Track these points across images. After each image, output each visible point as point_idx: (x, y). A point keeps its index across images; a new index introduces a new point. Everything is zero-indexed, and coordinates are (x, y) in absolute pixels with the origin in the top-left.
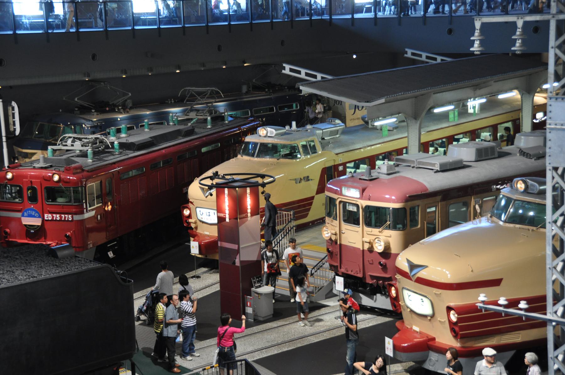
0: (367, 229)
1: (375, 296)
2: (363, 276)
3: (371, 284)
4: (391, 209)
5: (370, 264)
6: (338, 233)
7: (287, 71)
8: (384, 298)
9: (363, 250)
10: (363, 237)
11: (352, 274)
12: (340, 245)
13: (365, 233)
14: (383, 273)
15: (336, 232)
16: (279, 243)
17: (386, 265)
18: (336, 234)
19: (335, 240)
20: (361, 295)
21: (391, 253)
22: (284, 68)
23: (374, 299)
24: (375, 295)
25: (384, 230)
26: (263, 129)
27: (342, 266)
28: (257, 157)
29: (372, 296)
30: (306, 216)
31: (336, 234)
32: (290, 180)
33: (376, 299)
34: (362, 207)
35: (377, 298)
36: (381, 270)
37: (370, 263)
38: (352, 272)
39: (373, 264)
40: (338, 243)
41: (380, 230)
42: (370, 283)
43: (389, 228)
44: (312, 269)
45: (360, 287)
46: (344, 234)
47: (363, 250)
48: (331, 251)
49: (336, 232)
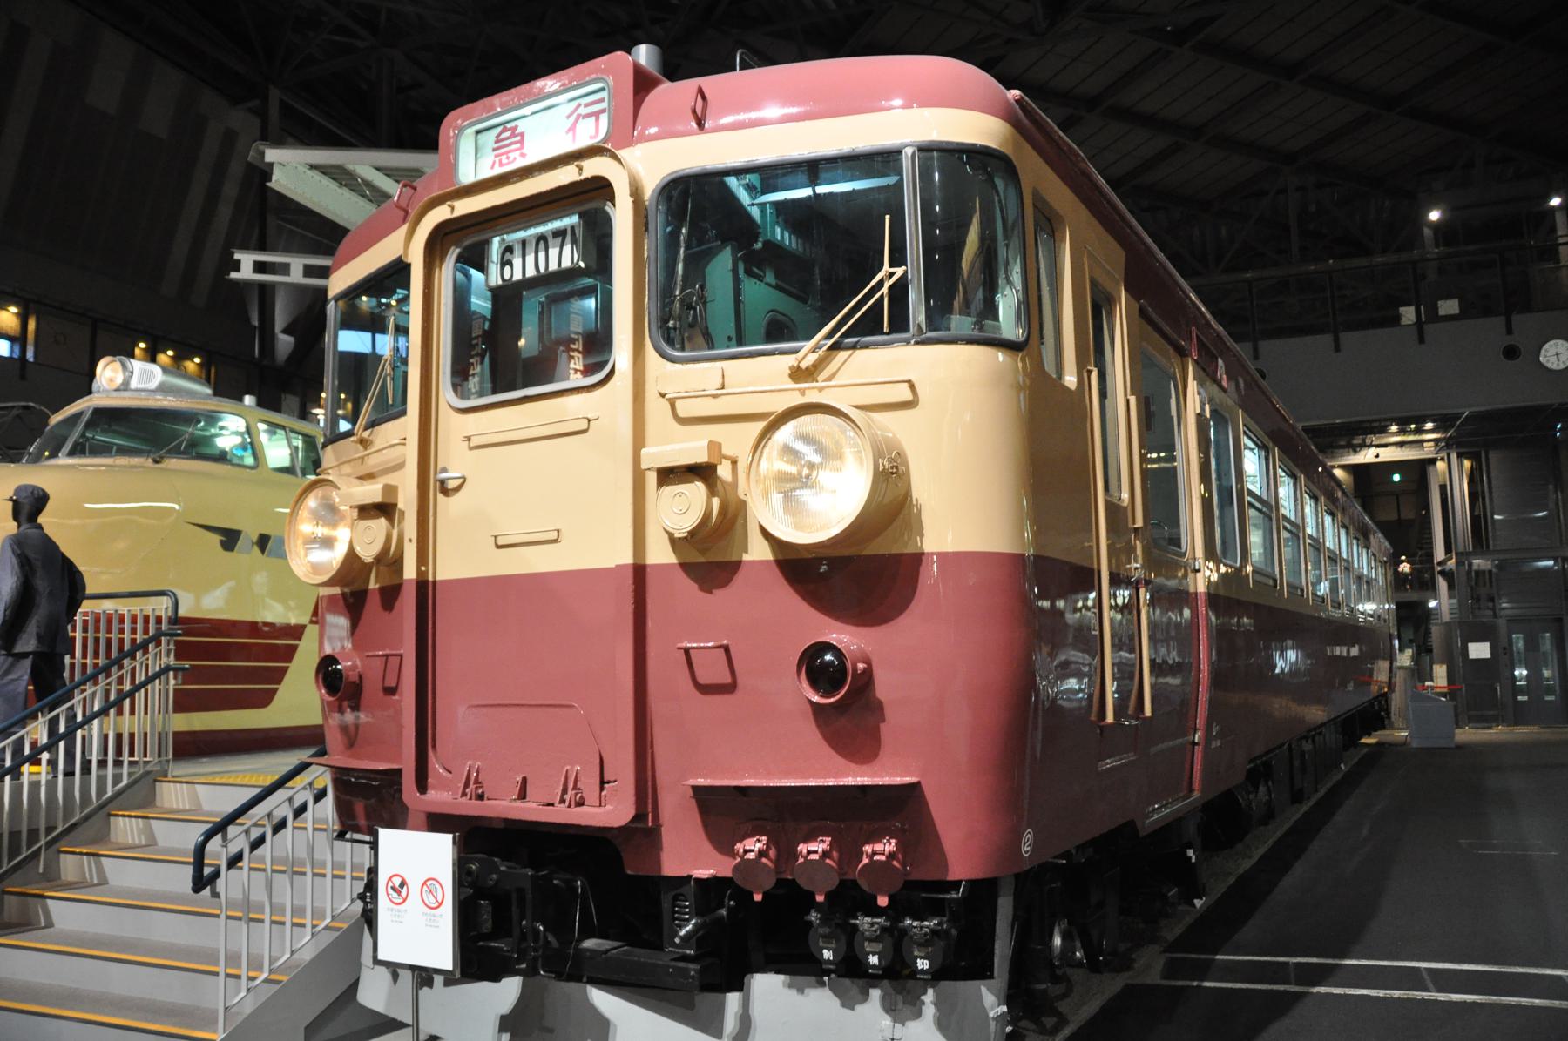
0: (665, 374)
1: (733, 1000)
2: (639, 816)
3: (711, 889)
4: (908, 151)
5: (706, 689)
6: (407, 500)
7: (246, 272)
8: (820, 1001)
9: (640, 571)
10: (639, 441)
11: (530, 810)
12: (425, 589)
13: (656, 410)
14: (840, 761)
15: (390, 490)
16: (69, 737)
17: (865, 681)
18: (384, 509)
19: (379, 559)
20: (602, 1000)
21: (918, 558)
22: (237, 266)
23: (730, 1023)
24: (738, 985)
25: (843, 355)
26: (117, 365)
27: (436, 767)
28: (71, 454)
29: (705, 1000)
30: (263, 700)
31: (384, 509)
32: (194, 524)
33: (745, 1021)
34: (636, 193)
35: (757, 1010)
36: (810, 732)
37: (702, 680)
38: (522, 795)
39: (729, 688)
40: (410, 572)
41: (807, 352)
42: (703, 873)
43: (900, 323)
44: (209, 836)
45: (587, 933)
46: (454, 500)
47: (640, 571)
48: (353, 677)
49: (390, 490)
